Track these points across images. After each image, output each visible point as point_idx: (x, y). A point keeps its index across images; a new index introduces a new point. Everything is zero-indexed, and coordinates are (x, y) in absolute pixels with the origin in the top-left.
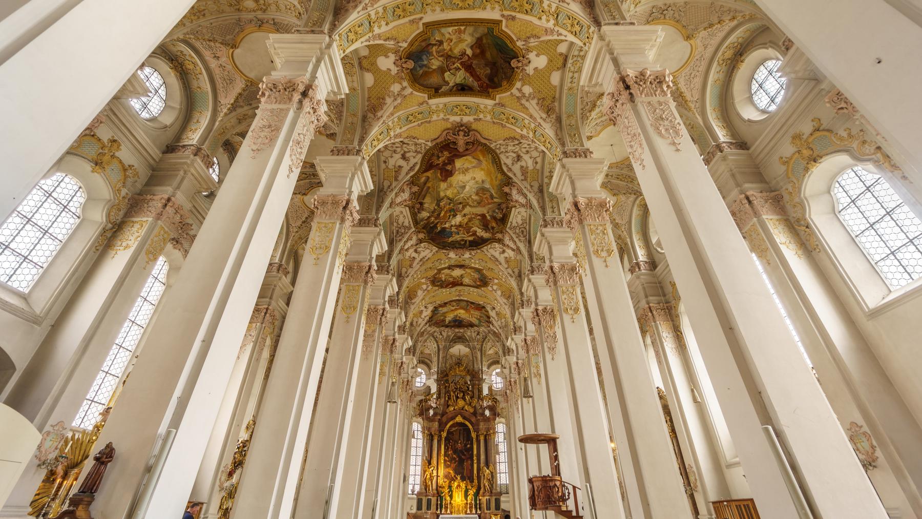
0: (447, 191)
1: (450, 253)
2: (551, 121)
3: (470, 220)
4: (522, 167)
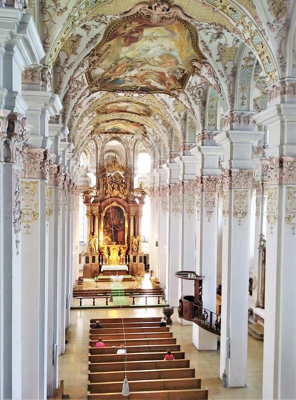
2: (278, 27)
4: (220, 44)
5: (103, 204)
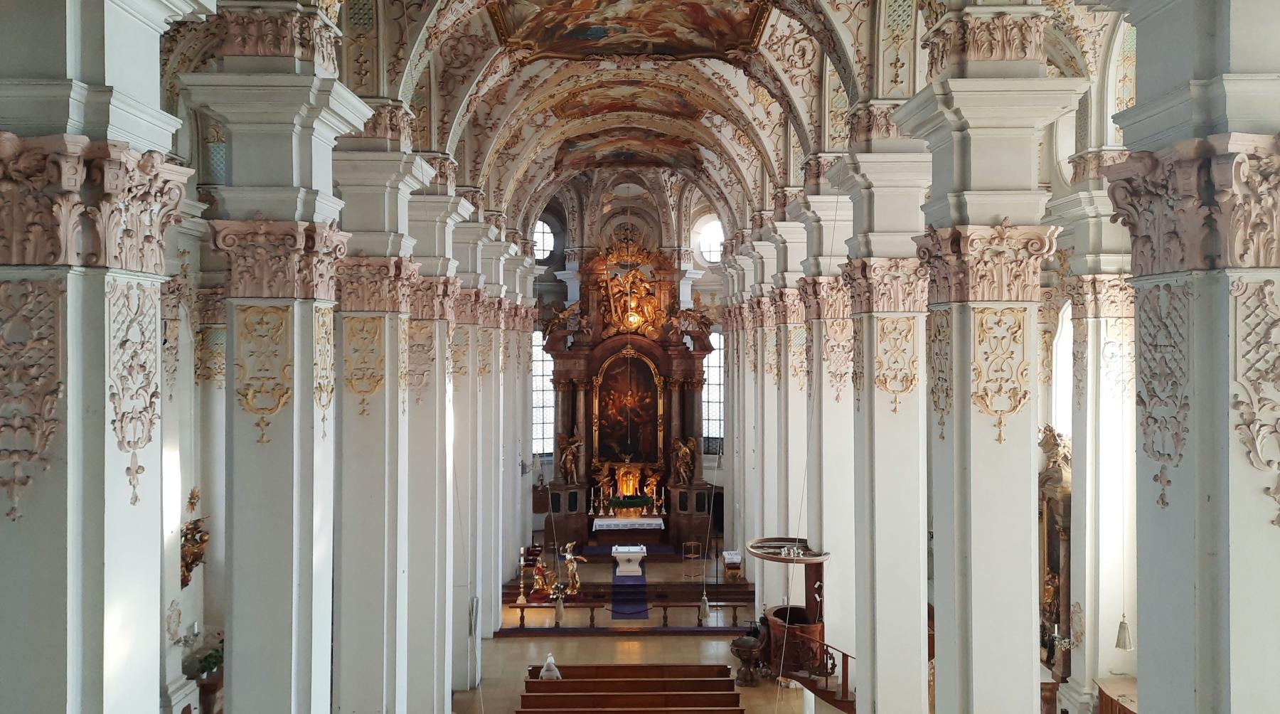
5: (598, 352)
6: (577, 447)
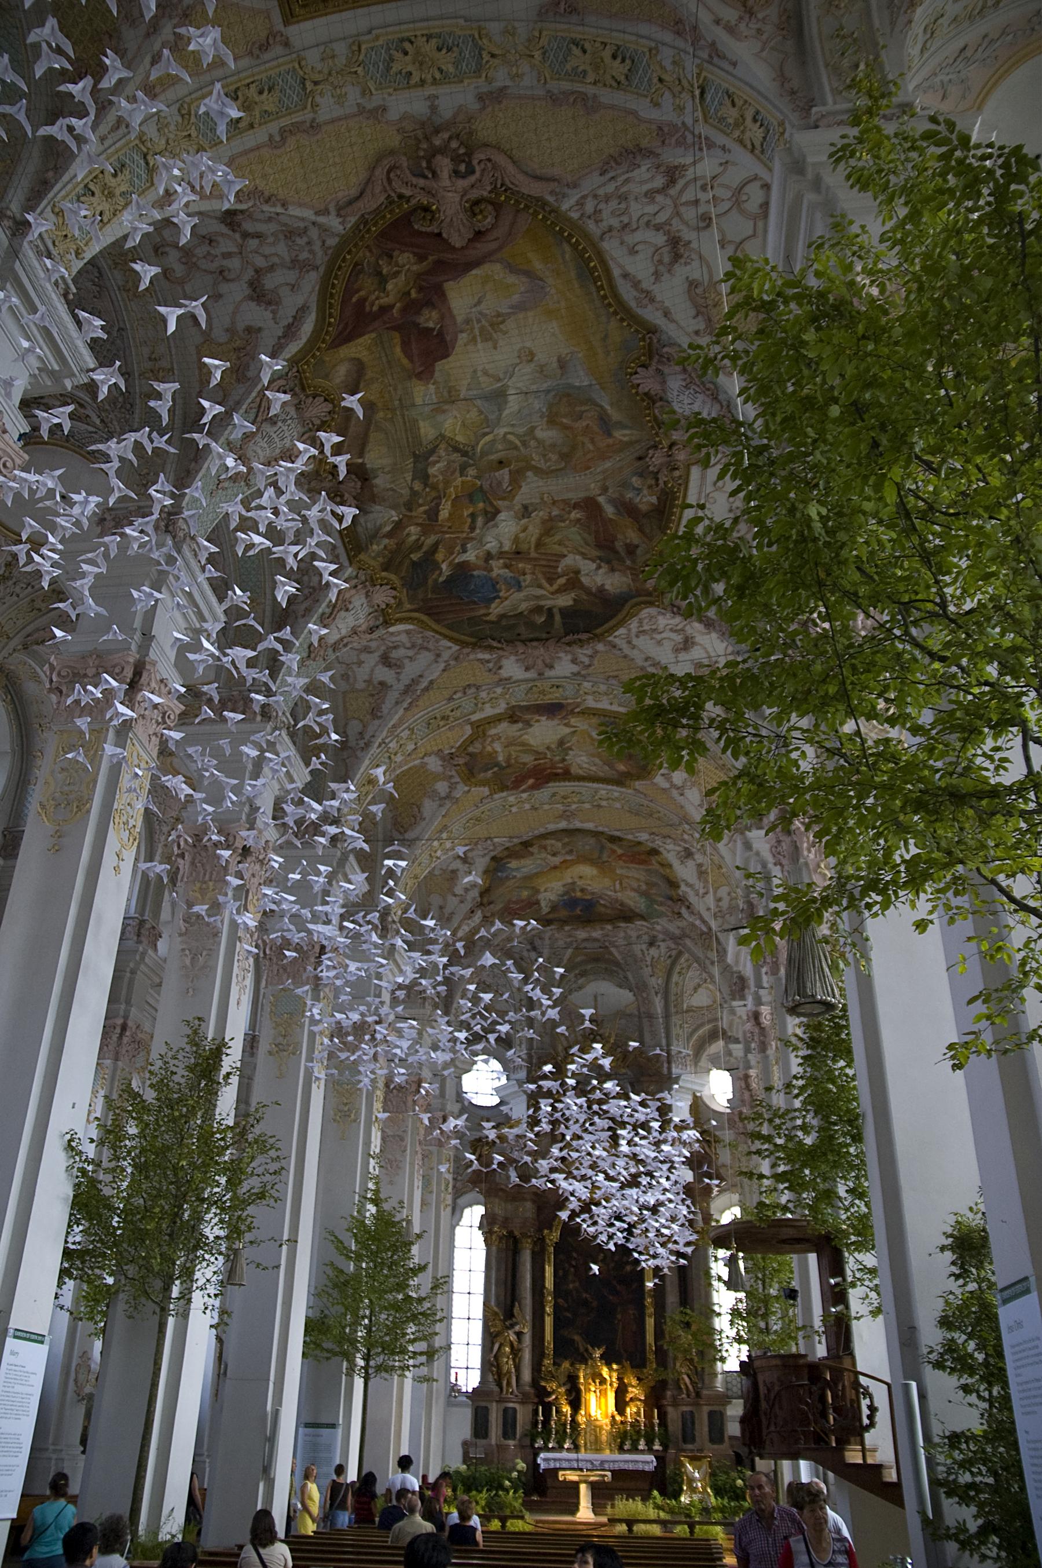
0: (440, 418)
1: (504, 662)
3: (549, 527)
4: (693, 285)
6: (519, 1334)
